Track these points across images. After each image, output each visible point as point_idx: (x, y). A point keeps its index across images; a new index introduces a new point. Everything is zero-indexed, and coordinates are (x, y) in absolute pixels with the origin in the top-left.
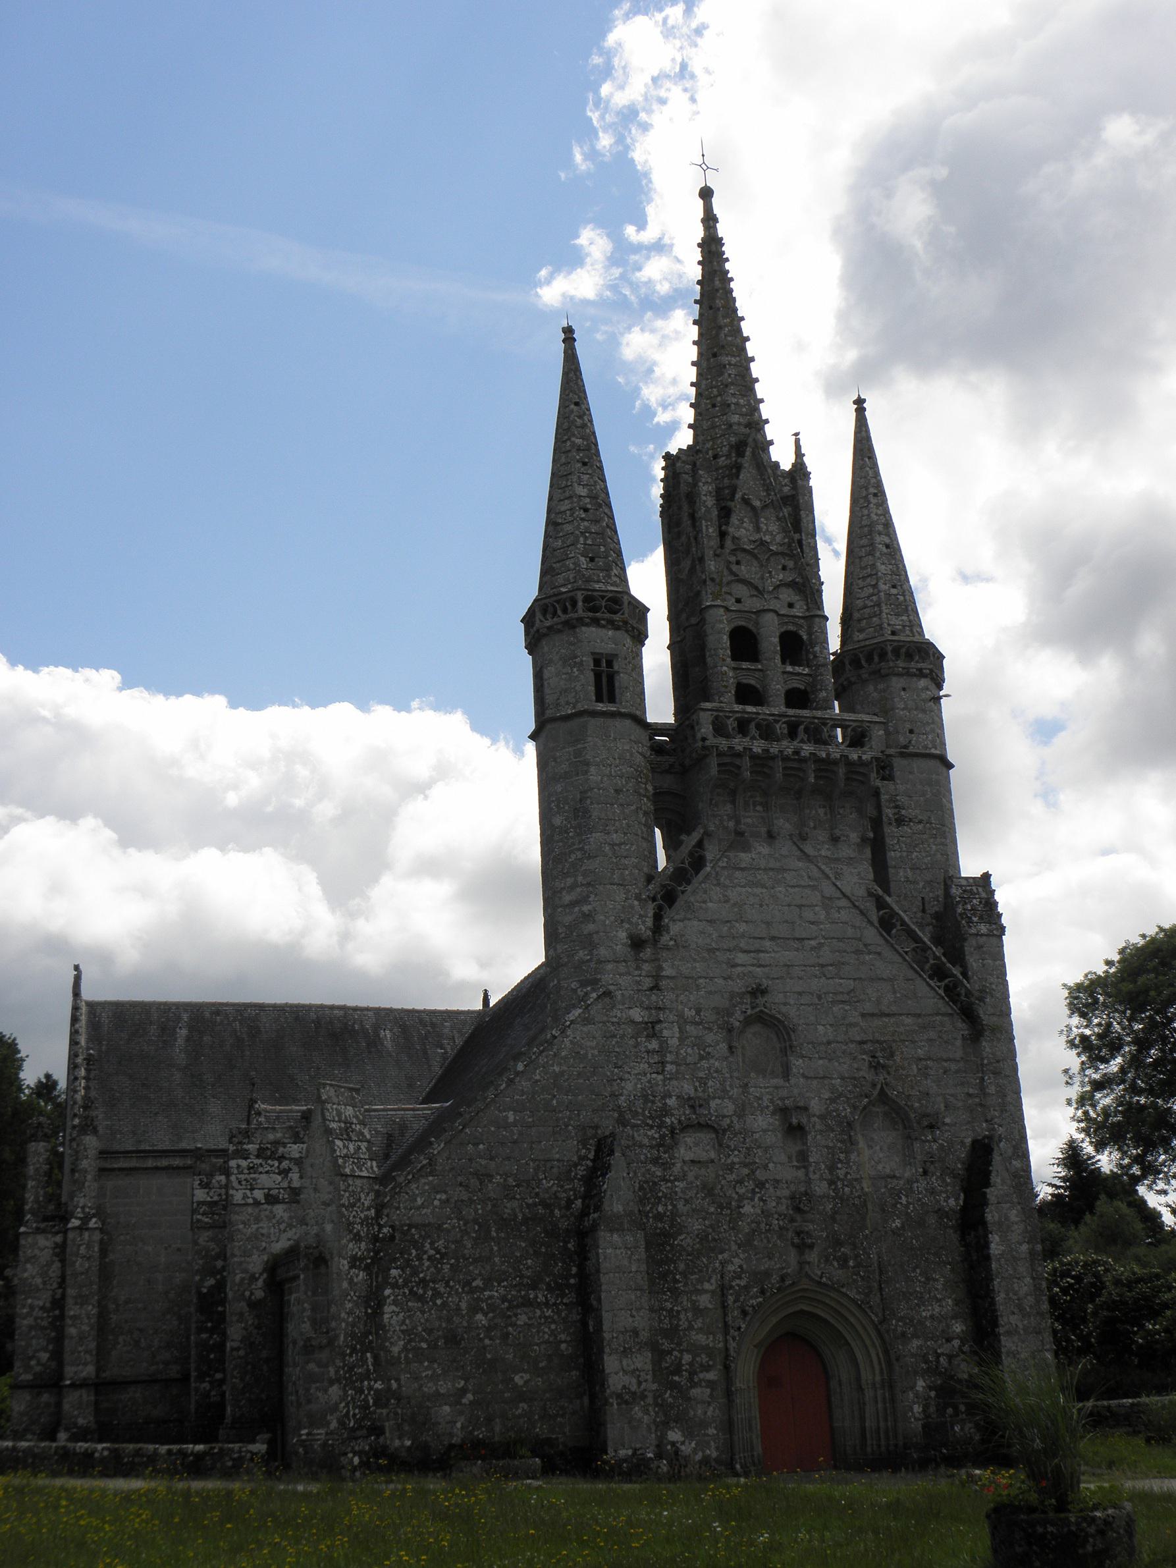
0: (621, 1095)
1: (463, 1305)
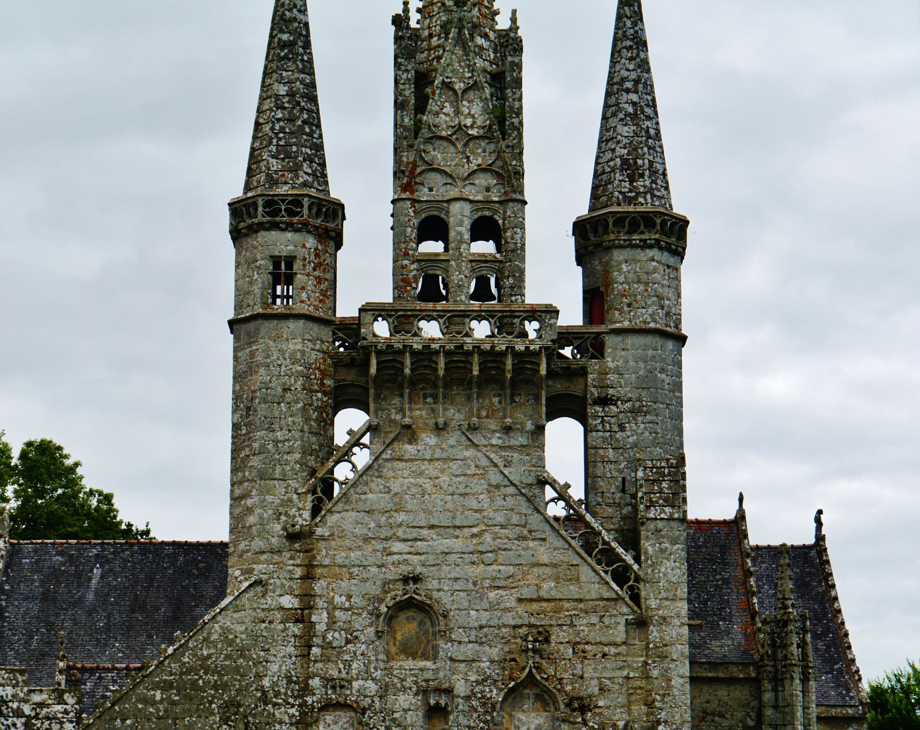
0: (266, 675)
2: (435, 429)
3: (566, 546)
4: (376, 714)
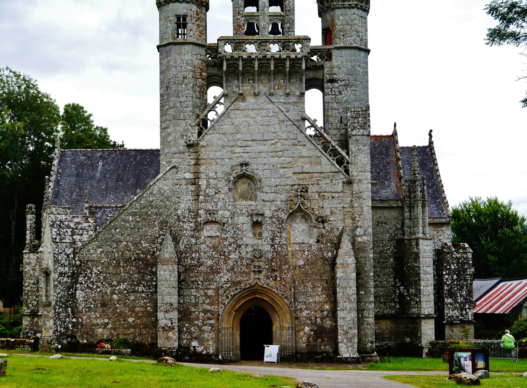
0: (179, 209)
1: (108, 291)
3: (315, 148)
4: (229, 225)
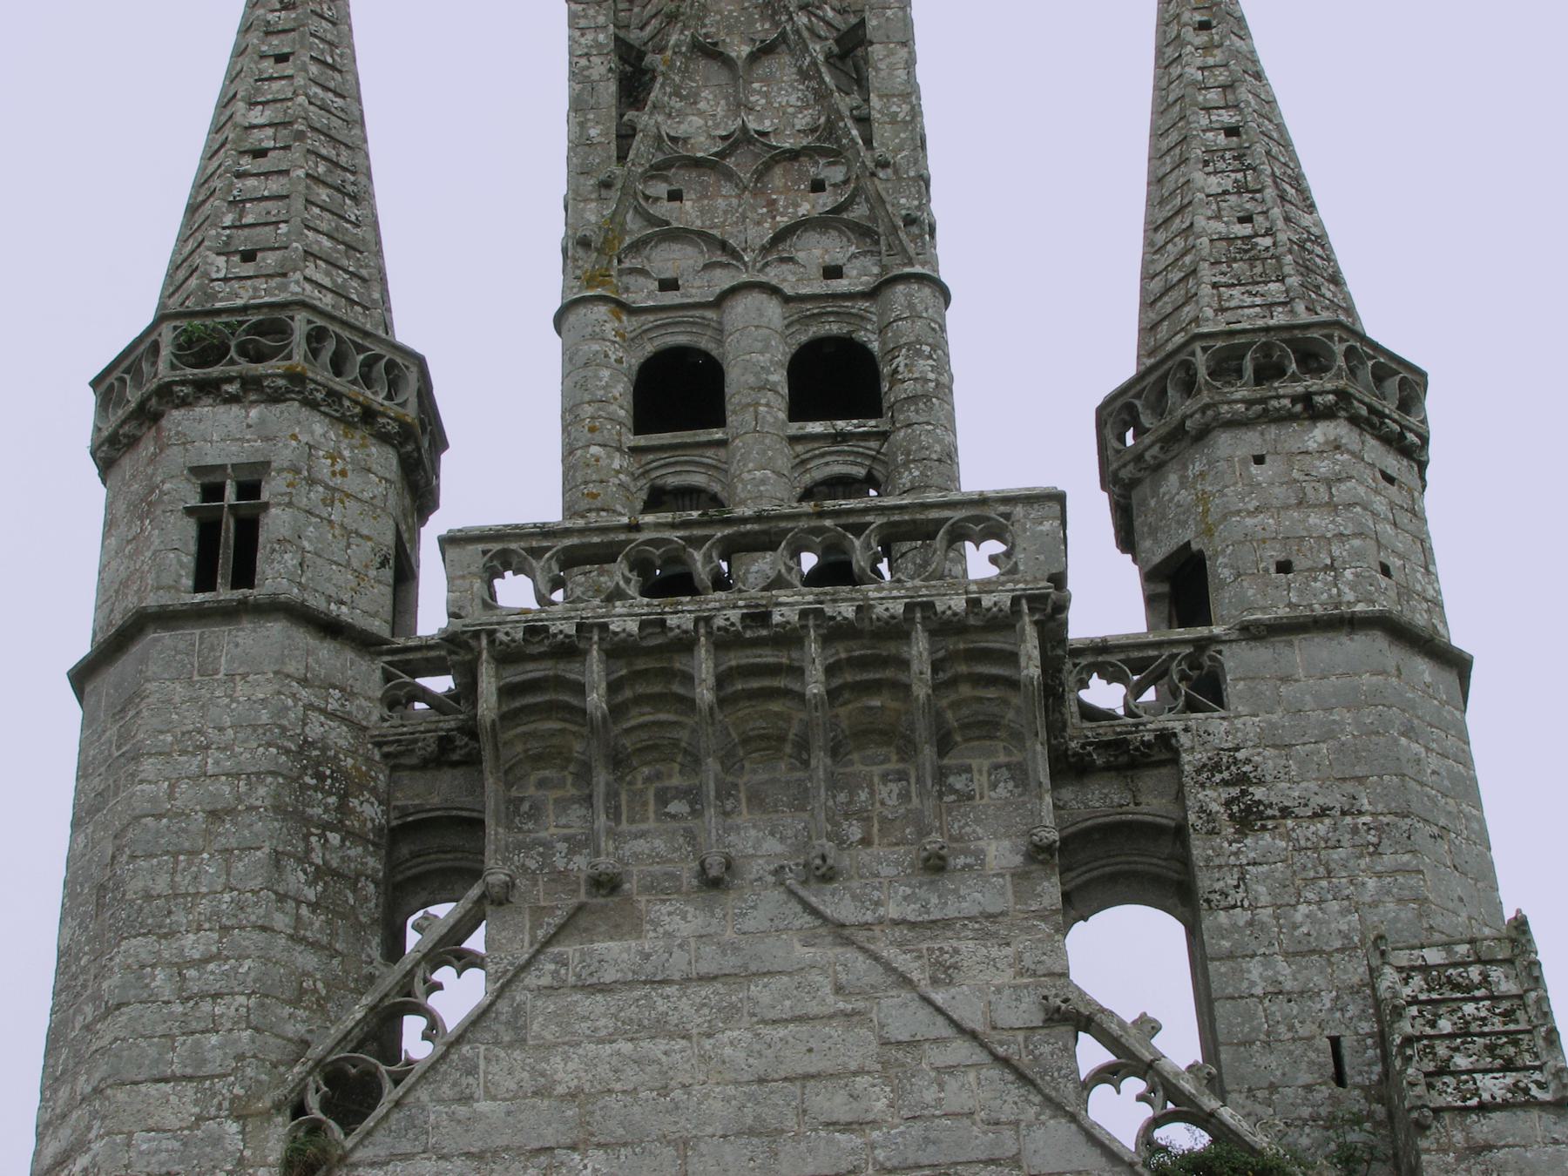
2: (700, 889)
